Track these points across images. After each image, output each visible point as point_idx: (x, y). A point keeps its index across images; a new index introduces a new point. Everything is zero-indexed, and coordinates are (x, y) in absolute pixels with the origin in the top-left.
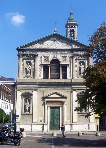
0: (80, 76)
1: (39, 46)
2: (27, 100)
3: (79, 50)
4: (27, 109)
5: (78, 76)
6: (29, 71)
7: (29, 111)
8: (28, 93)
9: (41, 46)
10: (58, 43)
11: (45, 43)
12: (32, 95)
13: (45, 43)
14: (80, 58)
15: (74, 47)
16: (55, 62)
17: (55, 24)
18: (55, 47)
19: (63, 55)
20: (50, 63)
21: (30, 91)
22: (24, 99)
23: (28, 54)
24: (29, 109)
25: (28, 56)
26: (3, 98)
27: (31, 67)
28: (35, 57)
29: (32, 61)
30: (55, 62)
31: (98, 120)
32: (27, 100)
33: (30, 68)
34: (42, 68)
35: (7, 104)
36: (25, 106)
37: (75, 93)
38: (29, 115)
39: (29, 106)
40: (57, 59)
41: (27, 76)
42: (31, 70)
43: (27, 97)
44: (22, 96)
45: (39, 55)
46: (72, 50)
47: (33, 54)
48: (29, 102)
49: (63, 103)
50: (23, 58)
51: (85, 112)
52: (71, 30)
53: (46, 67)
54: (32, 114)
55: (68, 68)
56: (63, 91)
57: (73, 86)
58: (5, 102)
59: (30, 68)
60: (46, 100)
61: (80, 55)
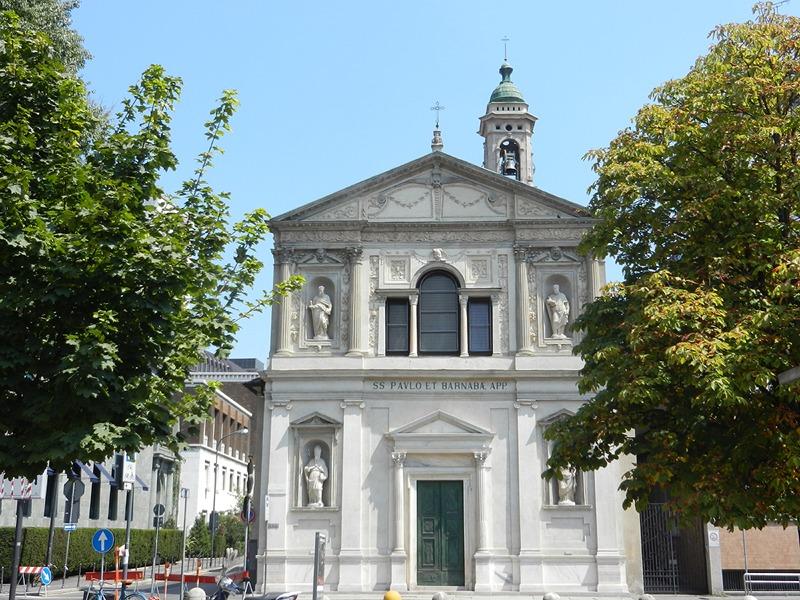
0: (550, 342)
1: (364, 210)
3: (543, 226)
4: (317, 490)
5: (540, 340)
6: (325, 320)
7: (326, 501)
9: (374, 210)
10: (452, 198)
11: (391, 199)
13: (391, 199)
14: (551, 260)
15: (524, 210)
16: (439, 277)
17: (434, 112)
18: (437, 213)
19: (474, 251)
20: (418, 286)
21: (329, 410)
22: (303, 442)
23: (320, 246)
24: (323, 492)
25: (320, 259)
27: (331, 306)
28: (349, 257)
29: (337, 277)
30: (439, 277)
33: (329, 310)
34: (382, 310)
36: (309, 474)
37: (527, 423)
39: (324, 477)
40: (446, 266)
41: (315, 344)
42: (330, 317)
43: (317, 439)
45: (366, 252)
46: (509, 226)
47: (341, 246)
48: (326, 457)
49: (476, 462)
50: (297, 264)
51: (574, 504)
53: (395, 303)
54: (338, 511)
55: (497, 309)
56: (470, 413)
57: (521, 386)
58: (222, 462)
59: (327, 307)
60: (399, 452)
61: (549, 249)
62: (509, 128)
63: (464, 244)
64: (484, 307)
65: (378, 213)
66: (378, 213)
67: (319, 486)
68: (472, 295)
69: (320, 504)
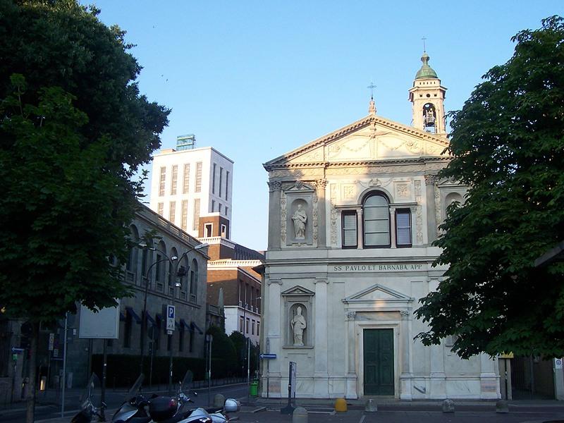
2: (299, 309)
8: (298, 288)
12: (313, 294)
19: (398, 179)
21: (307, 284)
26: (244, 306)
31: (509, 363)
32: (299, 309)
35: (251, 320)
36: (294, 325)
38: (306, 351)
44: (286, 295)
48: (304, 312)
52: (427, 106)
62: (428, 96)
63: (393, 175)
64: (406, 215)
65: (335, 156)
66: (335, 156)
67: (300, 332)
68: (397, 207)
69: (299, 343)
